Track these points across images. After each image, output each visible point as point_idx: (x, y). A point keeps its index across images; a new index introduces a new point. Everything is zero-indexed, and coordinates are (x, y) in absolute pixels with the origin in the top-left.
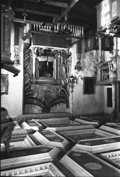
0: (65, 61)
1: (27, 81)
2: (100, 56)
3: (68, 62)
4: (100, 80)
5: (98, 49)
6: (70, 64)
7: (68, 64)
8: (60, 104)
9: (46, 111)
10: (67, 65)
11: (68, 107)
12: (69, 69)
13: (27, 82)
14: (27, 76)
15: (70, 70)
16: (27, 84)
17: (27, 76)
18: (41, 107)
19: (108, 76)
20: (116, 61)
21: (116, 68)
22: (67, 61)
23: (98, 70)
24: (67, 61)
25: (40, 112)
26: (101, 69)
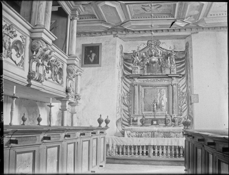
0: (123, 115)
1: (183, 83)
3: (120, 111)
6: (118, 109)
10: (121, 109)
13: (184, 80)
14: (184, 89)
15: (118, 98)
16: (184, 78)
17: (184, 89)
18: (161, 48)
21: (68, 79)
22: (121, 115)
24: (121, 115)
25: (161, 41)
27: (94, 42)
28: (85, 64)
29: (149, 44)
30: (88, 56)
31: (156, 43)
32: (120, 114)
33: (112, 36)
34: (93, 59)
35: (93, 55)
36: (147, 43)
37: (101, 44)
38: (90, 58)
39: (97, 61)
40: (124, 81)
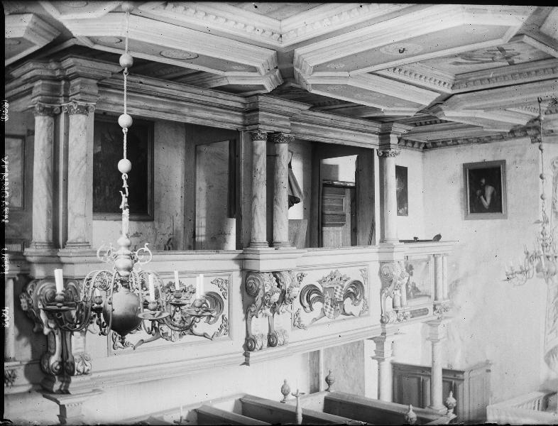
2: (438, 346)
4: (440, 259)
5: (444, 371)
19: (410, 269)
20: (382, 321)
23: (446, 296)
26: (436, 299)
27: (489, 159)
28: (472, 212)
30: (478, 192)
33: (528, 140)
34: (489, 199)
35: (489, 190)
37: (504, 162)
38: (482, 197)
39: (496, 206)
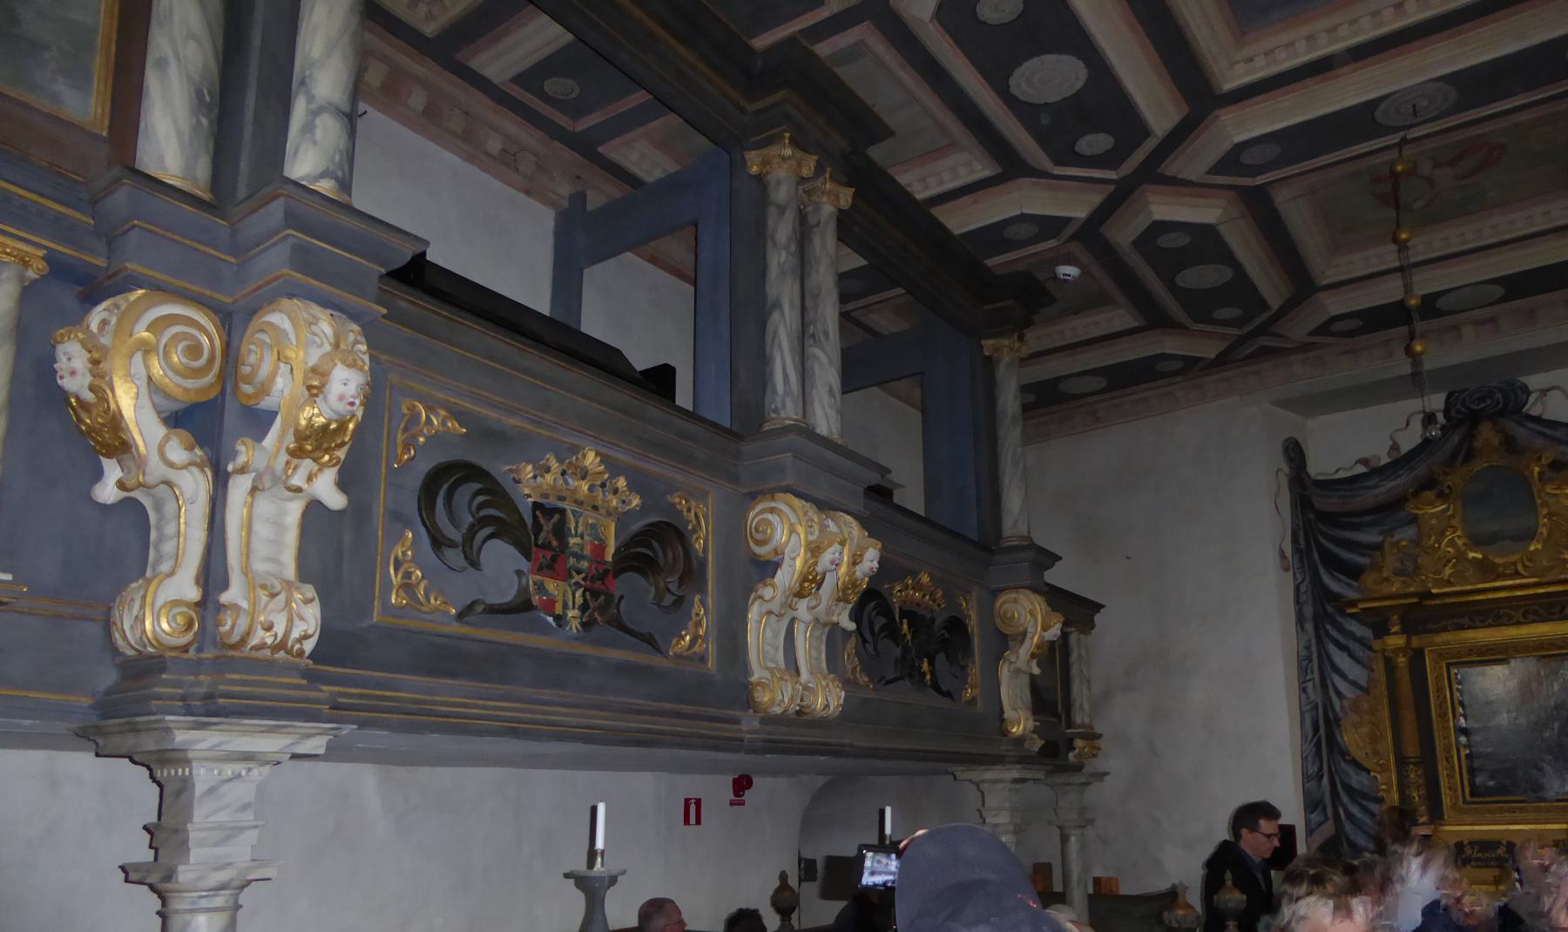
7: (1325, 780)
8: (1361, 469)
9: (1482, 399)
11: (1295, 453)
12: (1318, 746)
18: (1537, 420)
22: (1336, 814)
25: (1534, 381)
29: (1458, 411)
31: (1499, 395)
32: (1330, 811)
36: (1442, 406)
40: (1334, 633)
